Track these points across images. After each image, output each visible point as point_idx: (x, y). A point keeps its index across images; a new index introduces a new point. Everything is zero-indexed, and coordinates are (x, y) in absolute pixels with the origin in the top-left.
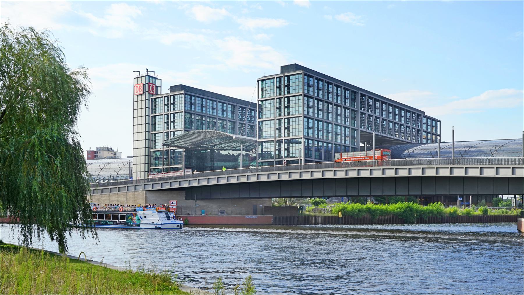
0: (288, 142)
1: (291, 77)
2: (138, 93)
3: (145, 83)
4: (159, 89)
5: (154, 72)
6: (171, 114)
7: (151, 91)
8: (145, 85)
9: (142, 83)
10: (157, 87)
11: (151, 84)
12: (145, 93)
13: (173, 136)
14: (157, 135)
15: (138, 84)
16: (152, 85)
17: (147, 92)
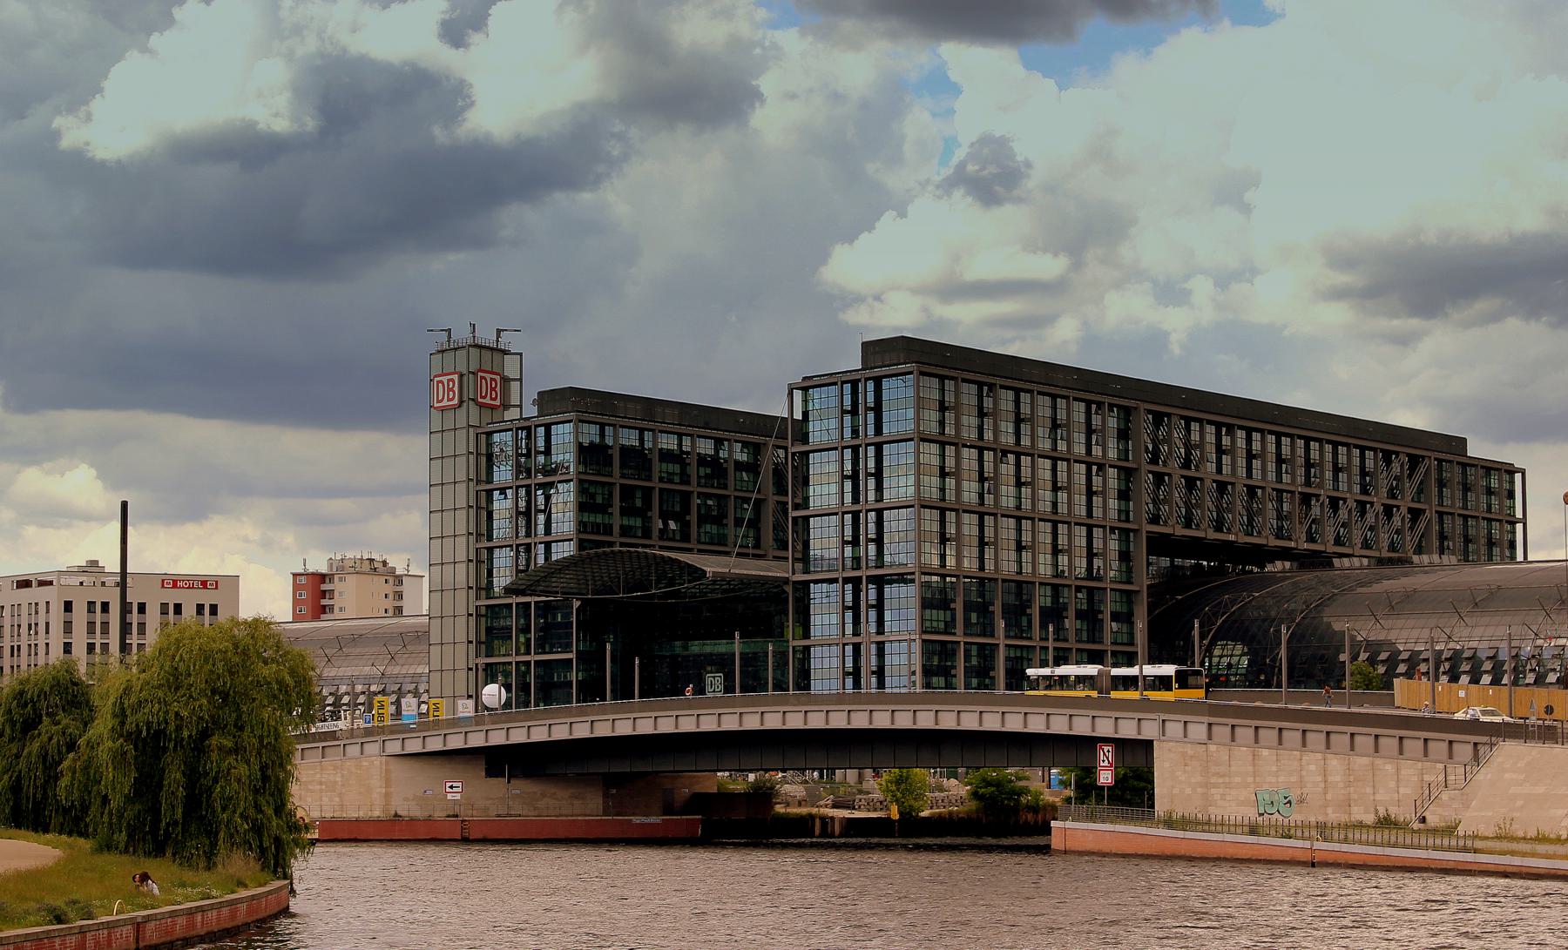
1: (885, 383)
2: (445, 403)
4: (515, 386)
5: (499, 331)
7: (485, 397)
8: (465, 378)
10: (506, 380)
12: (465, 404)
13: (547, 559)
14: (496, 552)
16: (488, 376)
17: (473, 400)
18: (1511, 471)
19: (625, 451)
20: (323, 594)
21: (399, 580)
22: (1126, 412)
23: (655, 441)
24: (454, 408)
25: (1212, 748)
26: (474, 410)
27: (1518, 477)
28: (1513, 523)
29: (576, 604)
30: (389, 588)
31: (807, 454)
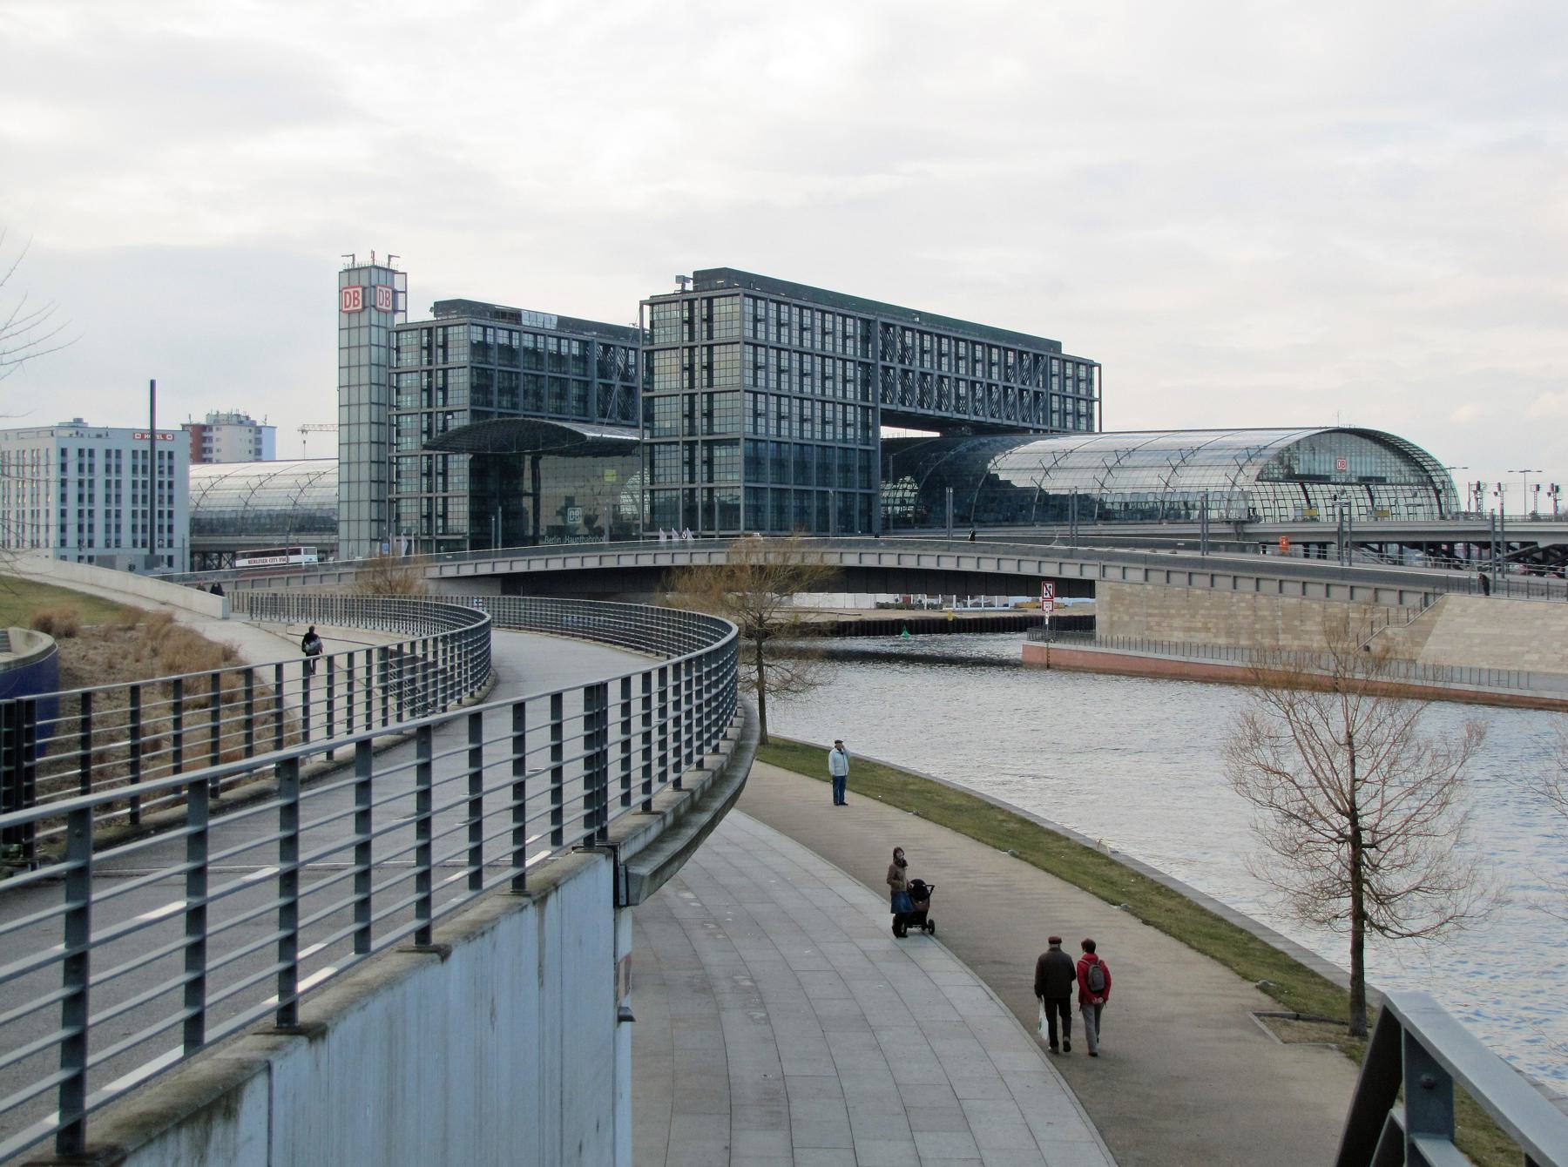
0: (710, 445)
1: (716, 301)
2: (351, 308)
4: (401, 297)
5: (390, 257)
6: (437, 370)
8: (367, 291)
9: (362, 283)
10: (395, 292)
11: (383, 286)
12: (367, 310)
15: (350, 287)
16: (384, 289)
18: (1090, 365)
19: (501, 346)
20: (204, 439)
21: (259, 430)
22: (866, 322)
23: (520, 340)
24: (359, 312)
25: (1149, 587)
26: (374, 313)
28: (1092, 401)
30: (251, 436)
31: (652, 352)
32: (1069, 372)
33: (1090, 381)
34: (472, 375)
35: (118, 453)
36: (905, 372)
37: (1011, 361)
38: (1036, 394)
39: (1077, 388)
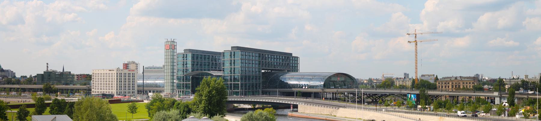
3: (170, 44)
4: (176, 46)
10: (175, 46)
18: (297, 57)
24: (169, 49)
27: (298, 58)
28: (298, 64)
29: (191, 76)
32: (294, 59)
33: (297, 60)
34: (192, 63)
35: (126, 73)
36: (266, 62)
37: (283, 58)
38: (288, 64)
39: (295, 62)
